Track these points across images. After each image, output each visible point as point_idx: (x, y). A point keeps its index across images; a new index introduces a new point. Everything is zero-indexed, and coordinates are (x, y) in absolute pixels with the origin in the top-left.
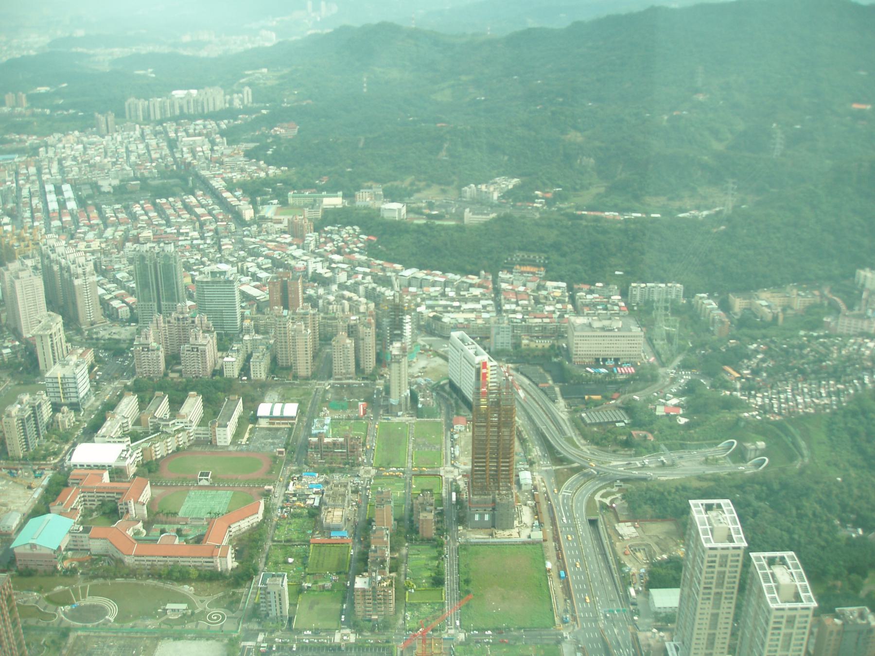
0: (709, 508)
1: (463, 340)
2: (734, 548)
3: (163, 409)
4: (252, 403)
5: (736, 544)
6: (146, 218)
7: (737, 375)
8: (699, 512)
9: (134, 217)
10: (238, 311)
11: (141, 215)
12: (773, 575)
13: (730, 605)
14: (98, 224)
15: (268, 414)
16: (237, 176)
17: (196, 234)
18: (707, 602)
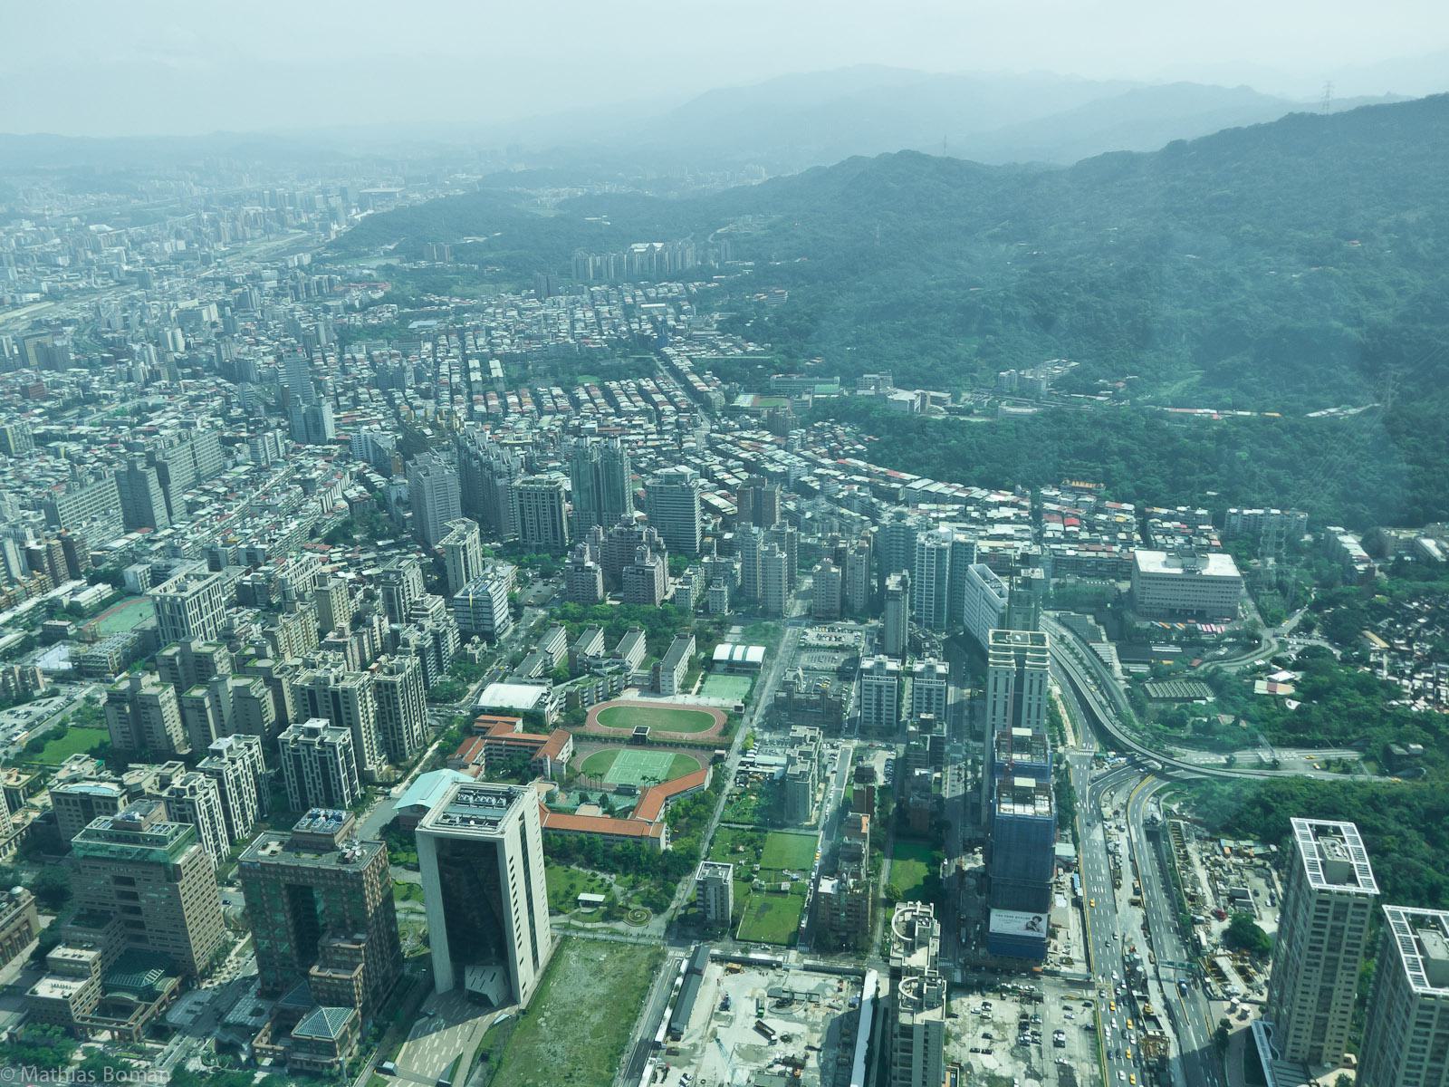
0: (1320, 832)
1: (985, 577)
2: (1357, 894)
3: (595, 645)
4: (707, 641)
5: (1362, 889)
6: (591, 405)
7: (1384, 645)
8: (1305, 837)
9: (576, 403)
10: (698, 525)
11: (586, 401)
12: (1419, 942)
13: (1350, 979)
14: (531, 412)
15: (726, 657)
16: (706, 354)
17: (652, 427)
18: (1315, 969)
